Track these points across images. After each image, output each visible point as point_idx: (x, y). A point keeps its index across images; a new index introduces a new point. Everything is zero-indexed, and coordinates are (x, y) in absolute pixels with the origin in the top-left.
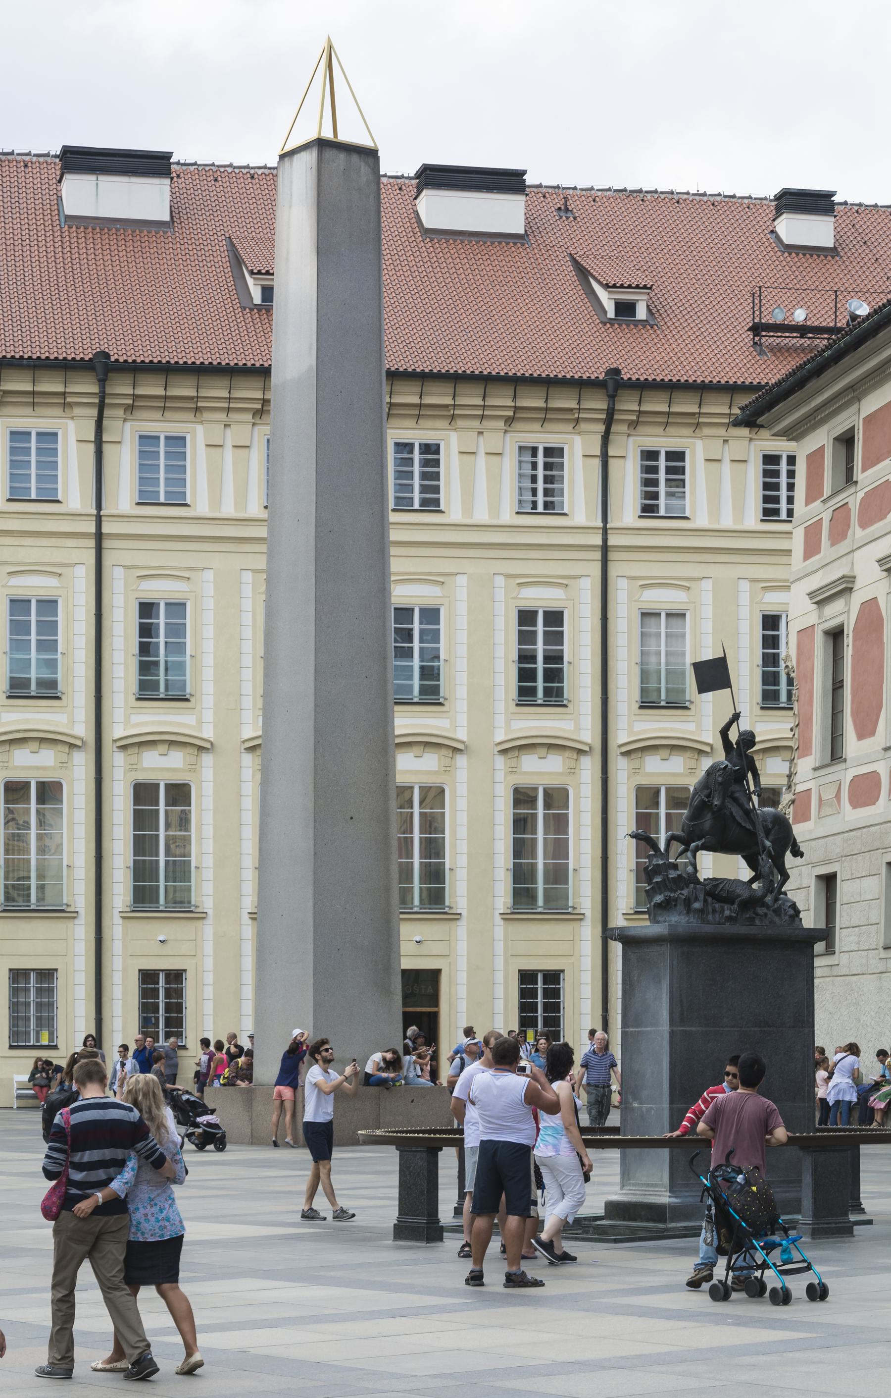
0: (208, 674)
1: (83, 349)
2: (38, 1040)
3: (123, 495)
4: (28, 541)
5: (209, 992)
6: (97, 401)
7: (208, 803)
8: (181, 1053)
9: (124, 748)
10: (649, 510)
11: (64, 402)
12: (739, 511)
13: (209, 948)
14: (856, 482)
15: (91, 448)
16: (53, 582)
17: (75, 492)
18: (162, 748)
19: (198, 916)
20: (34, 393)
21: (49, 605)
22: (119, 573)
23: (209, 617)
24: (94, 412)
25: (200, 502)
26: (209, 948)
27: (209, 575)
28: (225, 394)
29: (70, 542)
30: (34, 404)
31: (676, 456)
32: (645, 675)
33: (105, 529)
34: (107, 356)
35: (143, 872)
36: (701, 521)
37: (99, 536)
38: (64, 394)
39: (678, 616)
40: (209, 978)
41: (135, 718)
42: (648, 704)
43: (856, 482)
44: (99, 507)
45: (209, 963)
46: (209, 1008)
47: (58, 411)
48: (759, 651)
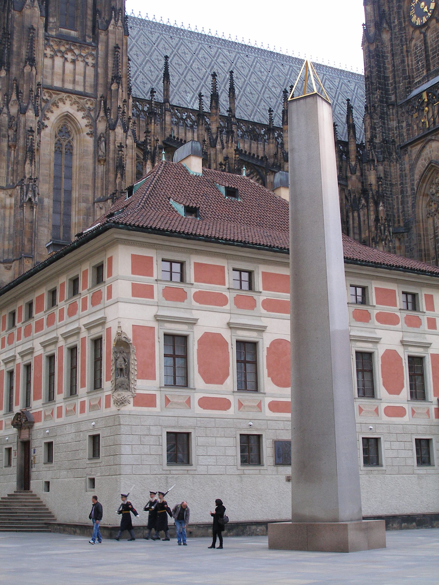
14: (105, 282)
43: (105, 282)
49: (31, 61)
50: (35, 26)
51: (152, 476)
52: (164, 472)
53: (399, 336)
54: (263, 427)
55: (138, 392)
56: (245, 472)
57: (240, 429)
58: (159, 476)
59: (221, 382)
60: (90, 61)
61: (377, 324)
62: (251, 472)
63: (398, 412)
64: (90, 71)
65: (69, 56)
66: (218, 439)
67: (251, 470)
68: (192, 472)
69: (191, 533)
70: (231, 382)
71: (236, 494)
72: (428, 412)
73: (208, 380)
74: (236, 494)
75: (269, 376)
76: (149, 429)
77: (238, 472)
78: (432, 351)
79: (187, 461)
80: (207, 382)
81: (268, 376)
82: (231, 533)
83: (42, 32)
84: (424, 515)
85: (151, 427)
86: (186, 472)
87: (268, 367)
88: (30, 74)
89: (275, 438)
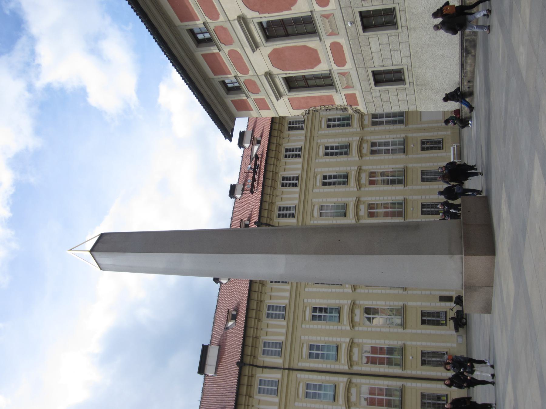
0: (330, 339)
1: (236, 370)
2: (444, 401)
3: (278, 361)
4: (289, 391)
5: (429, 344)
6: (251, 367)
7: (370, 303)
8: (448, 353)
9: (351, 366)
10: (293, 216)
11: (251, 376)
12: (294, 193)
13: (414, 343)
15: (265, 370)
16: (301, 384)
17: (276, 376)
18: (352, 354)
19: (404, 345)
20: (247, 385)
21: (308, 386)
22: (300, 364)
23: (314, 338)
24: (254, 368)
25: (282, 338)
26: (414, 343)
27: (302, 337)
28: (252, 329)
29: (290, 378)
30: (251, 386)
31: (280, 209)
32: (338, 216)
33: (287, 367)
34: (238, 363)
35: (390, 362)
36: (296, 202)
37: (289, 369)
38: (249, 376)
39: (322, 207)
40: (424, 344)
41: (343, 362)
42: (345, 215)
44: (280, 368)
45: (419, 343)
46: (433, 344)
47: (253, 379)
48: (332, 186)
51: (416, 94)
52: (412, 87)
54: (351, 12)
55: (346, 103)
56: (404, 24)
57: (358, 33)
58: (416, 90)
59: (315, 51)
62: (403, 19)
66: (373, 49)
67: (401, 19)
68: (410, 68)
69: (469, 82)
70: (311, 43)
71: (429, 33)
73: (318, 61)
74: (429, 33)
75: (291, 9)
76: (375, 97)
77: (405, 29)
79: (400, 72)
81: (291, 9)
82: (473, 51)
85: (374, 96)
86: (410, 73)
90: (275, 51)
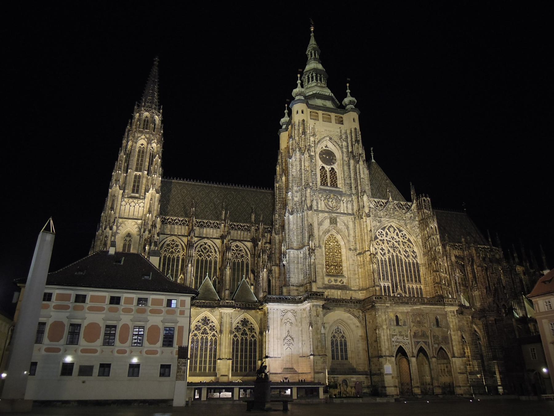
49: (112, 208)
50: (116, 195)
53: (162, 318)
59: (58, 341)
60: (142, 205)
61: (149, 314)
63: (155, 352)
64: (141, 209)
65: (133, 204)
72: (172, 353)
78: (179, 324)
80: (51, 341)
83: (120, 196)
84: (154, 400)
87: (84, 335)
88: (111, 214)
89: (81, 364)
90: (65, 325)
